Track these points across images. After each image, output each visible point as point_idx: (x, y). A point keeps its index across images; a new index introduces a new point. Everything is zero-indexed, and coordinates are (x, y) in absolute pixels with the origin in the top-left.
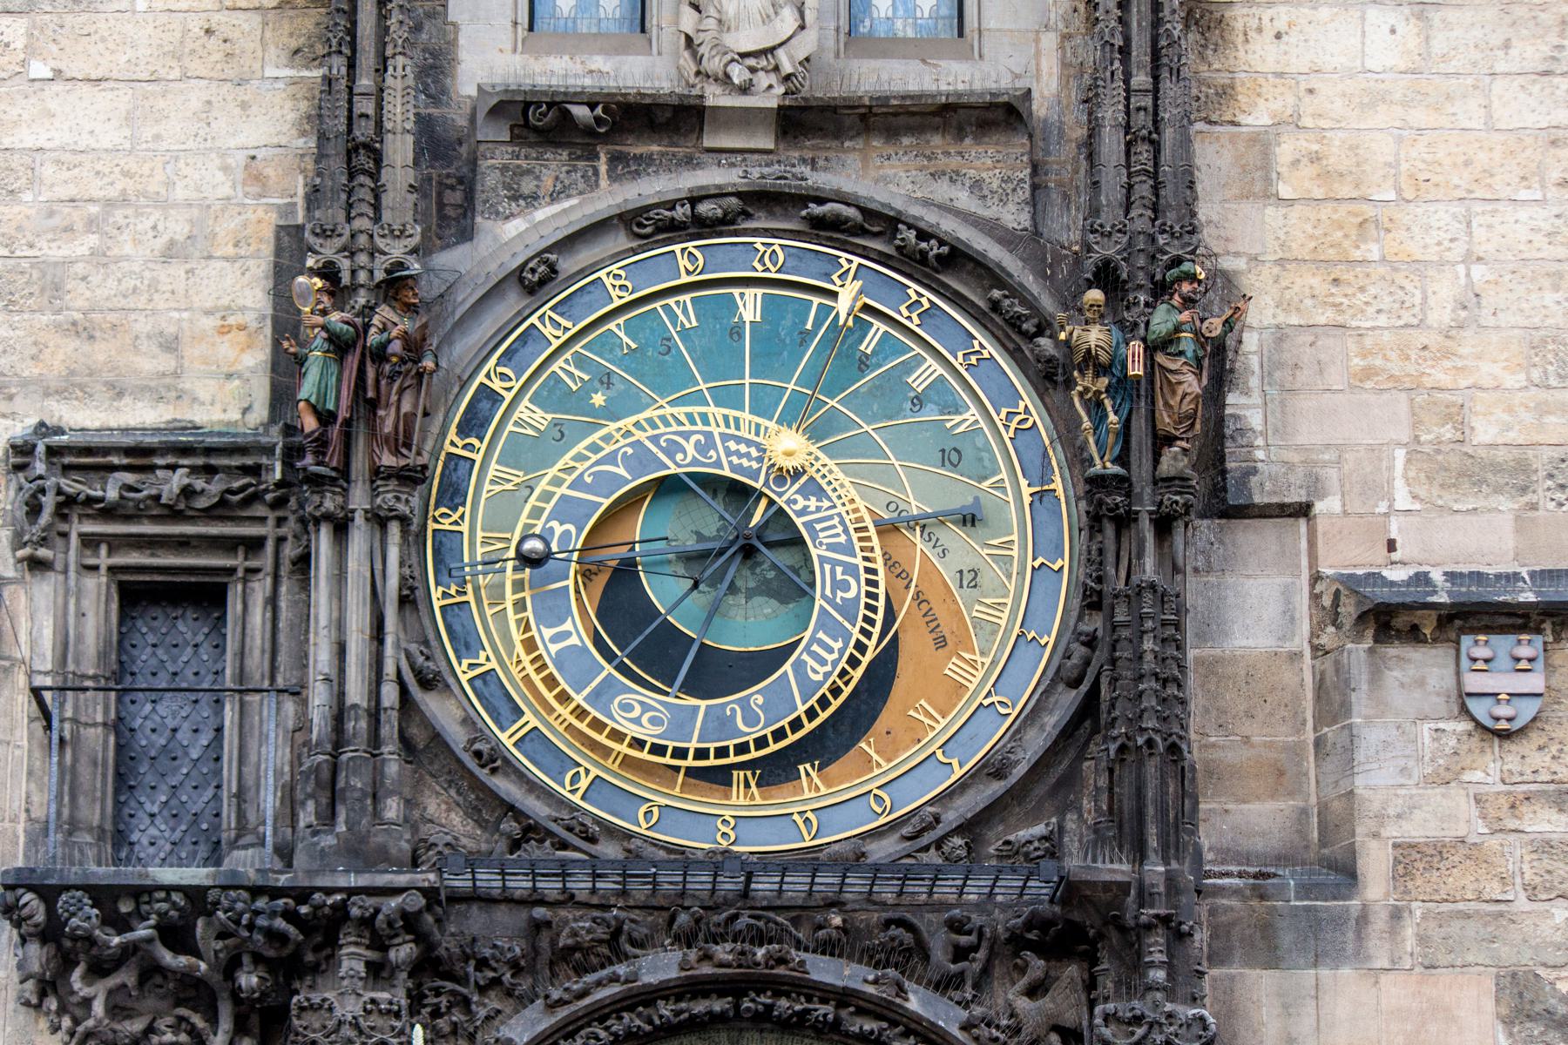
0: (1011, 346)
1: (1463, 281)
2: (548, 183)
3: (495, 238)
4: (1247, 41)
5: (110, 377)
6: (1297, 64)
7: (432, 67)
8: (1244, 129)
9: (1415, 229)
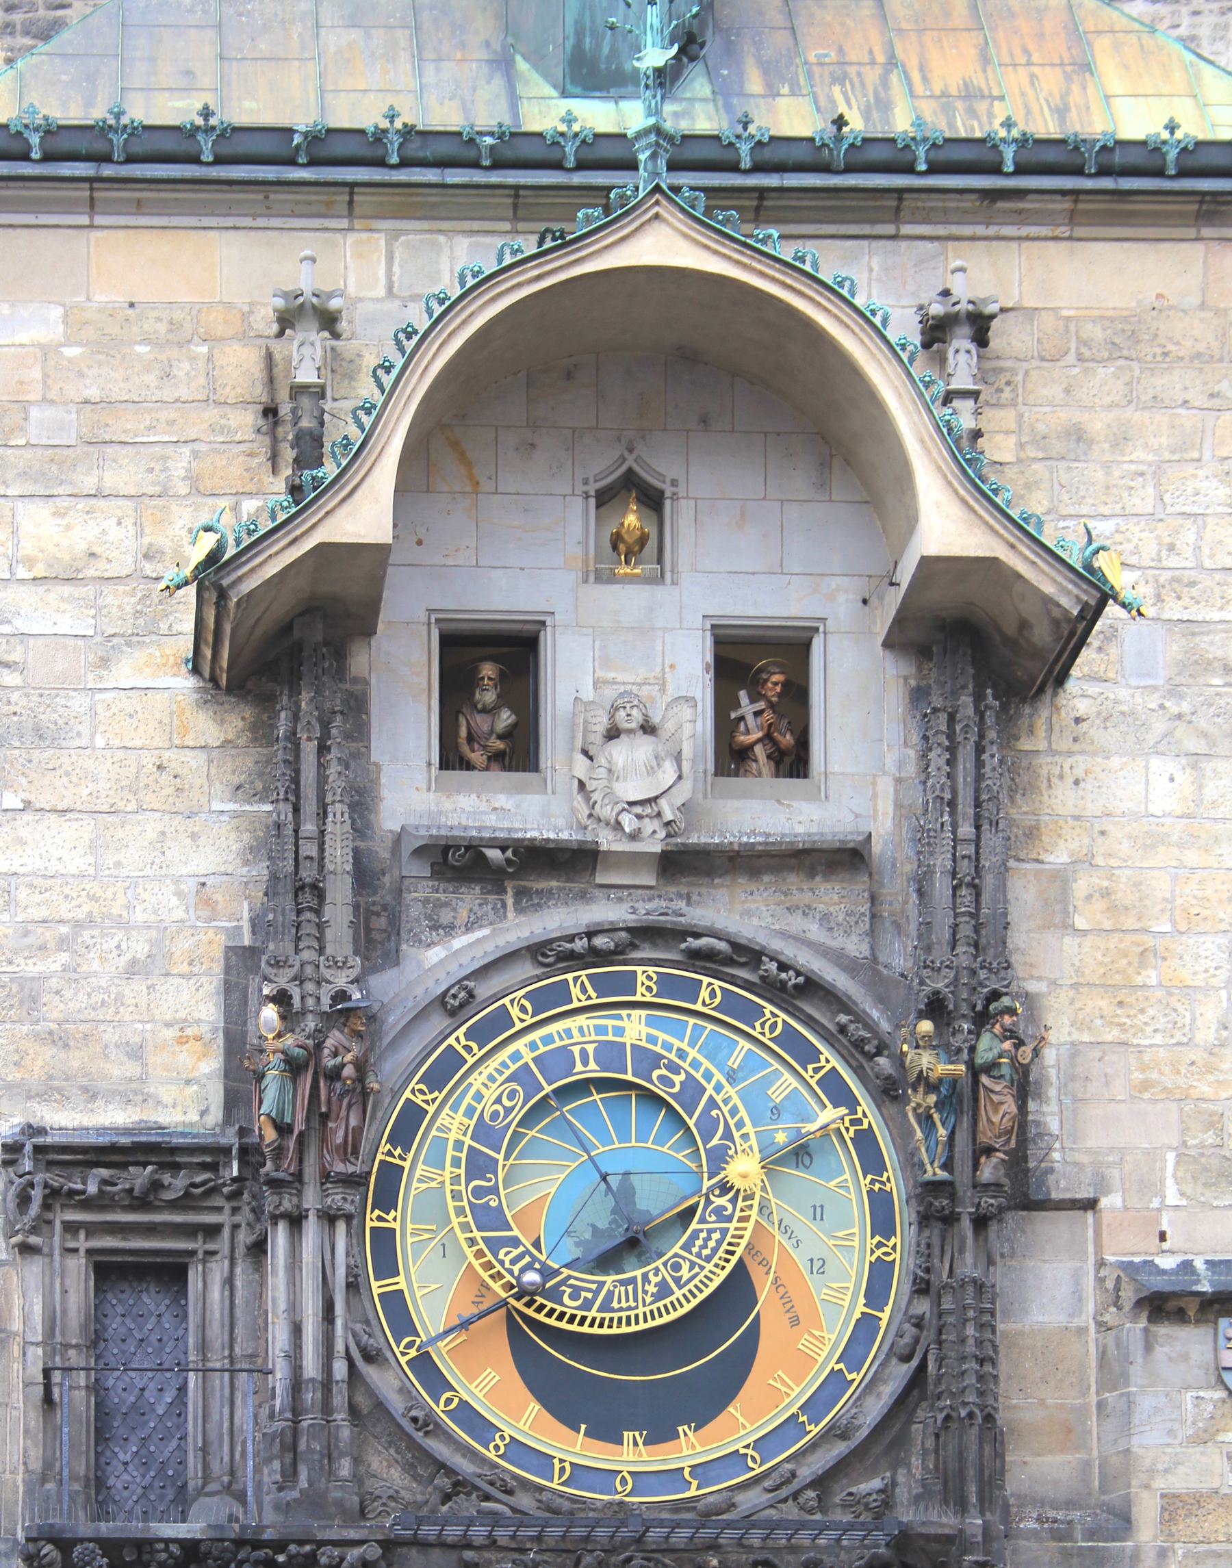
0: (854, 1063)
1: (1225, 1004)
2: (463, 914)
3: (419, 964)
4: (1050, 787)
5: (85, 1082)
6: (1092, 808)
7: (359, 803)
8: (1047, 866)
9: (1187, 958)
